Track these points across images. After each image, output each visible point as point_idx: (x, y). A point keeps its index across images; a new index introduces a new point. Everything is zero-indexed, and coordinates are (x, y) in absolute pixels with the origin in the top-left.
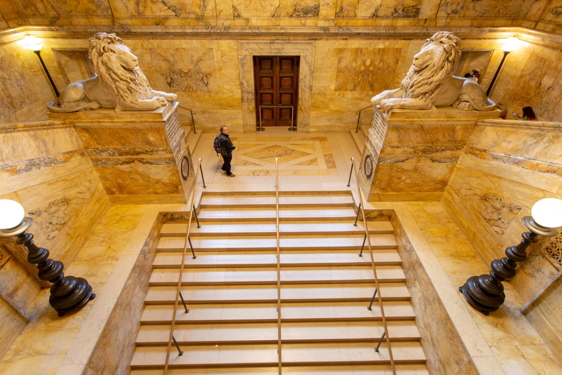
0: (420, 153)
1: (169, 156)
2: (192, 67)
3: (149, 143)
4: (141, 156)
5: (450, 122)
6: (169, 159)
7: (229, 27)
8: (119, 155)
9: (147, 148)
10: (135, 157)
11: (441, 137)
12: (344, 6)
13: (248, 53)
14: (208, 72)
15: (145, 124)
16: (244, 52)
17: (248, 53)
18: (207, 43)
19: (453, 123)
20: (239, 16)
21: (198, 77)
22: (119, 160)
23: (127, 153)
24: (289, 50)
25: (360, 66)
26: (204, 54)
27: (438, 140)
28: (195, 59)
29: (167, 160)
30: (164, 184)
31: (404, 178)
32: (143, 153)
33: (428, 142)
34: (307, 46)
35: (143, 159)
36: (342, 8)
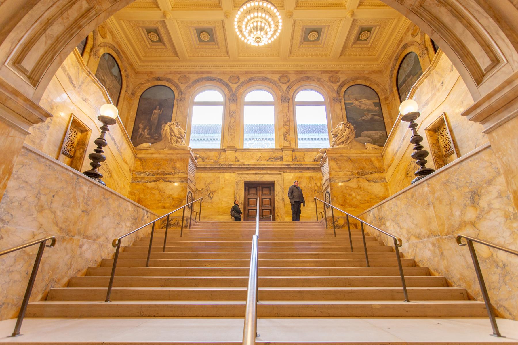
0: (357, 175)
1: (185, 176)
2: (204, 187)
3: (175, 168)
4: (165, 176)
5: (365, 155)
6: (184, 178)
7: (232, 165)
8: (153, 175)
9: (173, 171)
10: (162, 177)
11: (365, 165)
12: (297, 156)
13: (241, 179)
14: (214, 190)
15: (178, 155)
16: (239, 179)
17: (241, 179)
18: (217, 174)
19: (368, 155)
20: (238, 161)
21: (207, 193)
22: (150, 179)
23: (158, 174)
24: (267, 177)
25: (314, 186)
26: (214, 180)
27: (364, 167)
28: (207, 183)
29: (183, 179)
30: (173, 199)
31: (354, 195)
32: (168, 174)
33: (359, 169)
34: (278, 176)
35: (166, 178)
36: (296, 158)
